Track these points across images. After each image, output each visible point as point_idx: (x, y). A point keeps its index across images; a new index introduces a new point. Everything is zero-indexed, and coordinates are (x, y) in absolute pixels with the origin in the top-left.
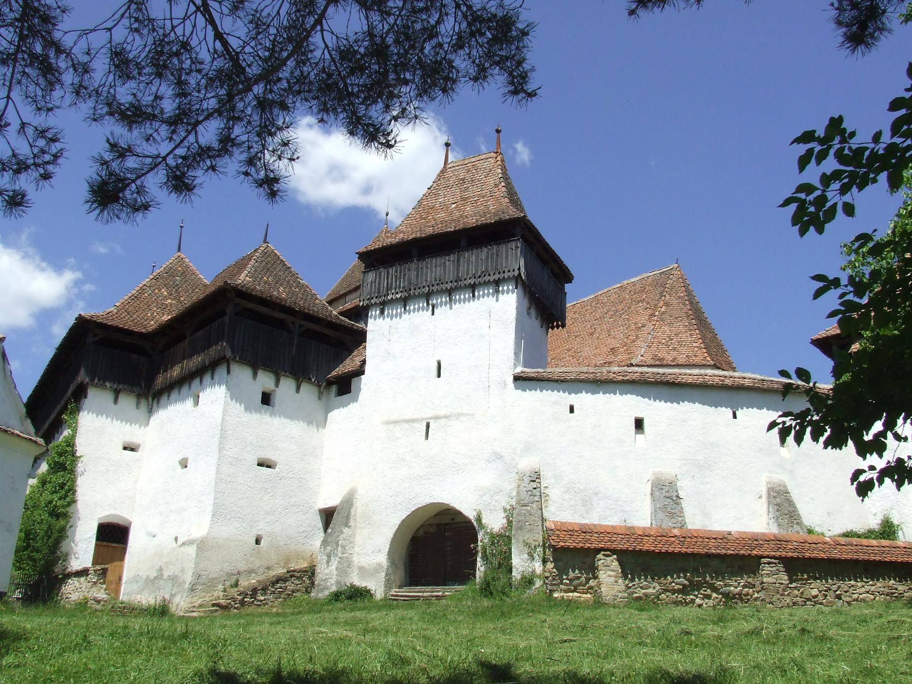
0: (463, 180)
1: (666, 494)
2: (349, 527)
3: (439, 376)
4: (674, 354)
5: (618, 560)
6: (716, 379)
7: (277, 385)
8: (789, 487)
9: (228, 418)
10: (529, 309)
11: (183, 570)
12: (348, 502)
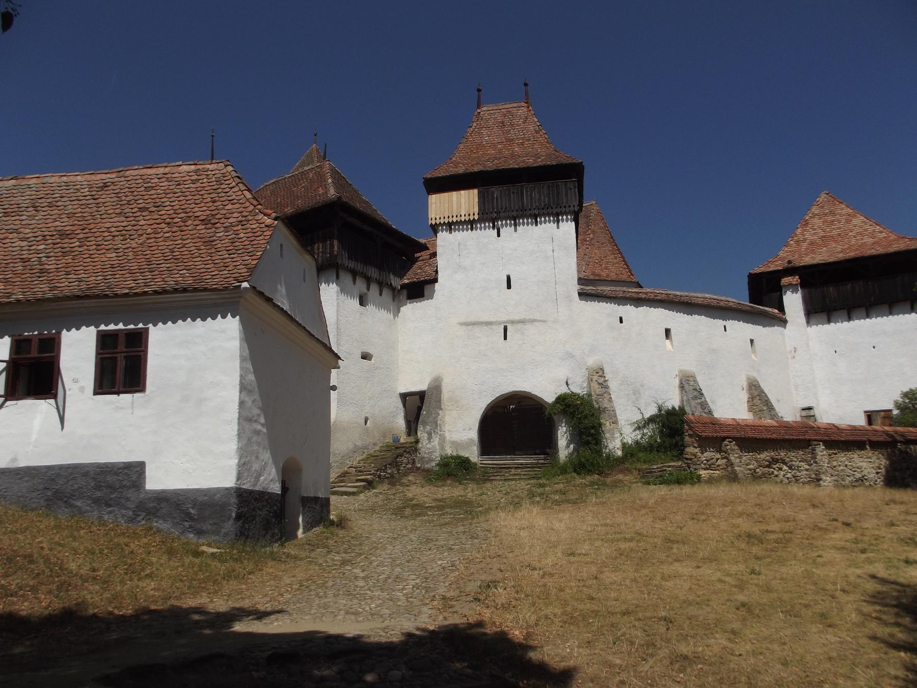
0: (503, 123)
3: (509, 287)
4: (607, 271)
5: (736, 444)
7: (368, 289)
9: (340, 318)
12: (436, 387)
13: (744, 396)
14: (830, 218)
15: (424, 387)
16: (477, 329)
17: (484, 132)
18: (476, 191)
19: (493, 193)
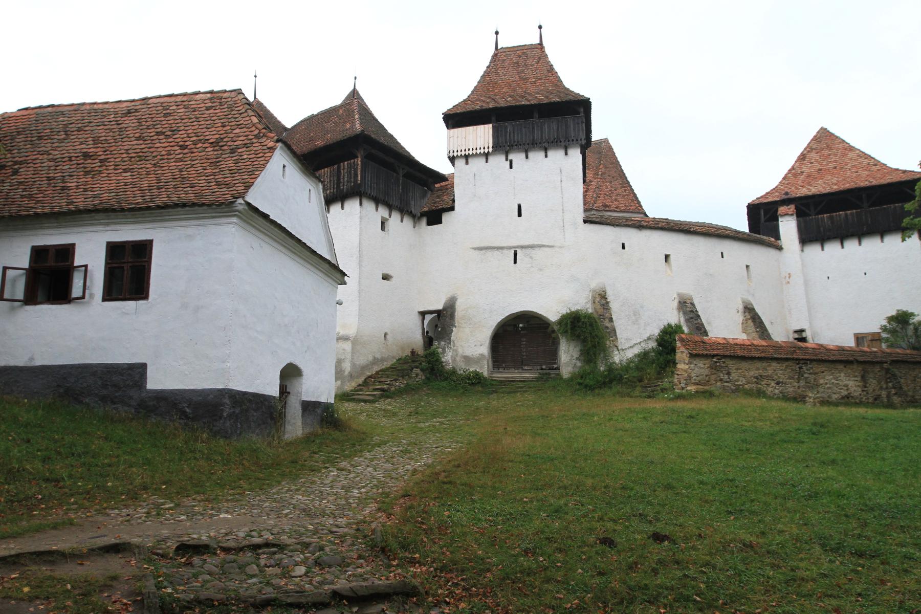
0: (517, 63)
3: (520, 215)
4: (616, 203)
7: (390, 216)
13: (740, 318)
14: (826, 152)
15: (440, 307)
16: (489, 253)
17: (500, 71)
18: (491, 125)
19: (506, 127)
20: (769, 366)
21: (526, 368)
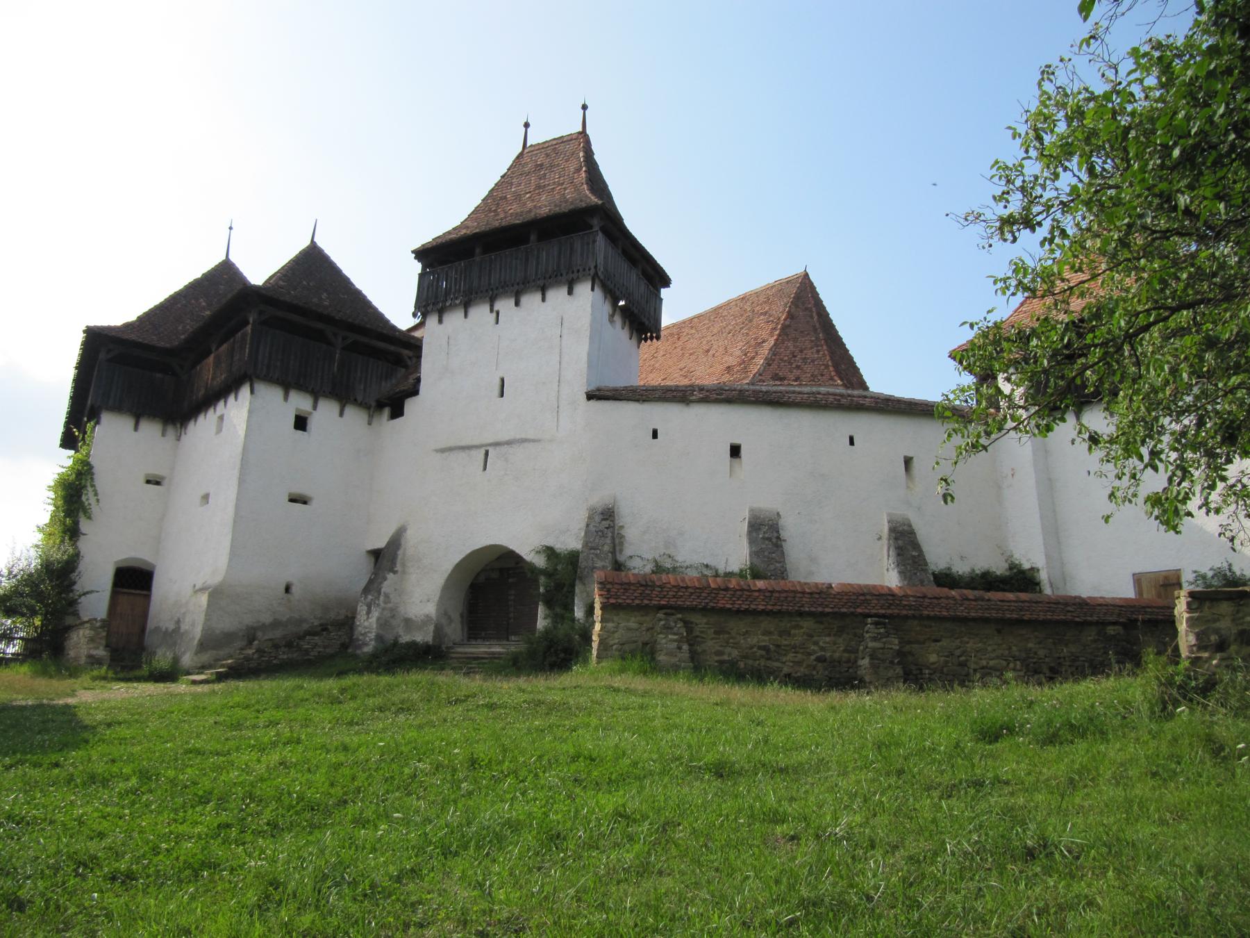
0: (541, 165)
1: (766, 533)
2: (395, 572)
3: (502, 395)
6: (831, 398)
7: (315, 408)
8: (914, 526)
10: (612, 316)
11: (193, 625)
12: (395, 542)
16: (453, 456)
20: (798, 627)
21: (513, 638)
